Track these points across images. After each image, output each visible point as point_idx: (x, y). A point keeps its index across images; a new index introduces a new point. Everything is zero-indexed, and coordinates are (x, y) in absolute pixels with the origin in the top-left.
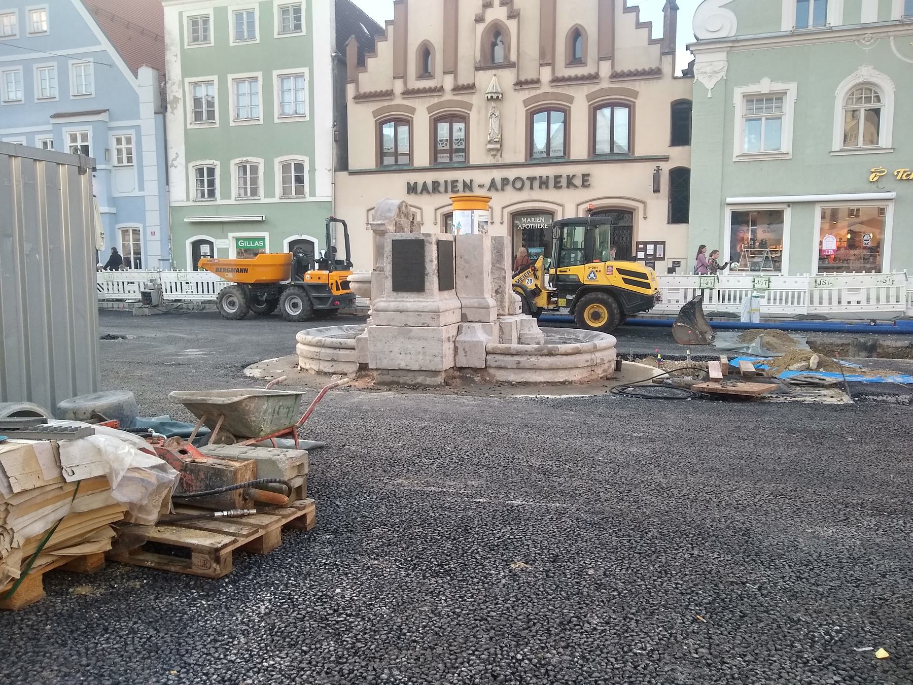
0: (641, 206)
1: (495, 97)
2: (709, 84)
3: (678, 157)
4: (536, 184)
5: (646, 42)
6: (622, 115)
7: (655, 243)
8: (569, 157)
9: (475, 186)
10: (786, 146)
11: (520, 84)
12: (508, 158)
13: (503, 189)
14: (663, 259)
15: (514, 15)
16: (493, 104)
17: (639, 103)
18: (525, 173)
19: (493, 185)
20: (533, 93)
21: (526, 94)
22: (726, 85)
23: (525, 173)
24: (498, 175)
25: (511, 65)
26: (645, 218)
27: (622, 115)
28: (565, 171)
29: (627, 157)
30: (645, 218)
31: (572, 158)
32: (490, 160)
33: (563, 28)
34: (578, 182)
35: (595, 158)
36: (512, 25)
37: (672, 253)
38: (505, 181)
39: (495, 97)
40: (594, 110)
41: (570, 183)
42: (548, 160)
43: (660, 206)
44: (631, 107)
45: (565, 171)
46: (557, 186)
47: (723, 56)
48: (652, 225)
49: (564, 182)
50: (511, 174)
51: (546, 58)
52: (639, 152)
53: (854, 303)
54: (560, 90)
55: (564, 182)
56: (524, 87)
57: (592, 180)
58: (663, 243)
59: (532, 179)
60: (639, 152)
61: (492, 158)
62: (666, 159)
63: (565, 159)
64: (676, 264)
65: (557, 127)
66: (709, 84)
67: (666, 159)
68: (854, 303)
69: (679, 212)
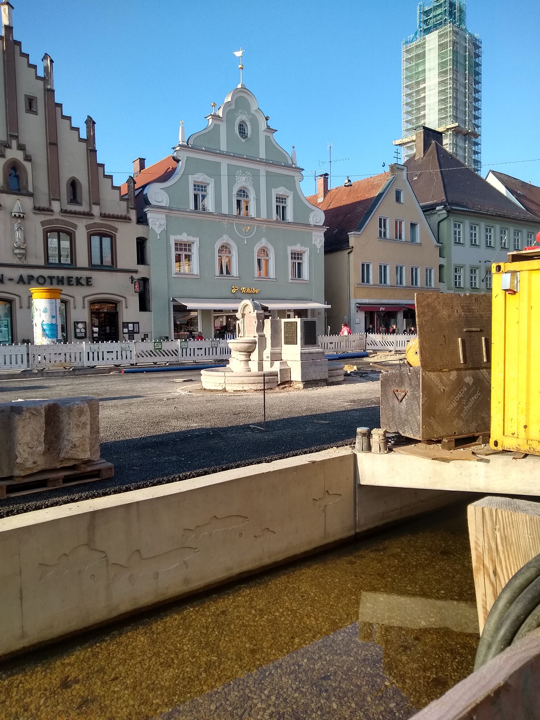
0: (123, 300)
1: (17, 215)
2: (158, 231)
3: (143, 271)
4: (55, 281)
5: (118, 199)
6: (106, 241)
7: (133, 323)
8: (76, 264)
9: (5, 281)
10: (196, 271)
11: (38, 210)
12: (31, 261)
13: (29, 283)
14: (138, 333)
15: (28, 158)
16: (19, 221)
17: (118, 235)
18: (46, 273)
19: (21, 280)
20: (48, 218)
21: (42, 218)
22: (167, 233)
23: (46, 273)
24: (25, 272)
25: (31, 195)
26: (127, 308)
27: (106, 241)
28: (75, 274)
29: (113, 268)
30: (127, 308)
31: (78, 265)
32: (16, 261)
33: (65, 177)
34: (83, 282)
35: (92, 267)
36: (28, 165)
37: (143, 329)
38: (31, 278)
39: (17, 215)
40: (90, 236)
41: (78, 282)
42: (60, 266)
43: (134, 301)
44: (112, 237)
45: (75, 274)
46: (69, 284)
47: (164, 216)
48: (129, 312)
49: (74, 281)
50: (36, 273)
51: (54, 196)
52: (120, 266)
53: (200, 355)
54: (67, 219)
55: (74, 281)
56: (42, 212)
57: (93, 281)
58: (138, 323)
59: (51, 278)
60: (120, 266)
61: (18, 259)
62: (136, 272)
63: (73, 266)
64: (146, 336)
65: (65, 244)
66: (158, 231)
67: (136, 272)
68: (200, 355)
69: (144, 306)
